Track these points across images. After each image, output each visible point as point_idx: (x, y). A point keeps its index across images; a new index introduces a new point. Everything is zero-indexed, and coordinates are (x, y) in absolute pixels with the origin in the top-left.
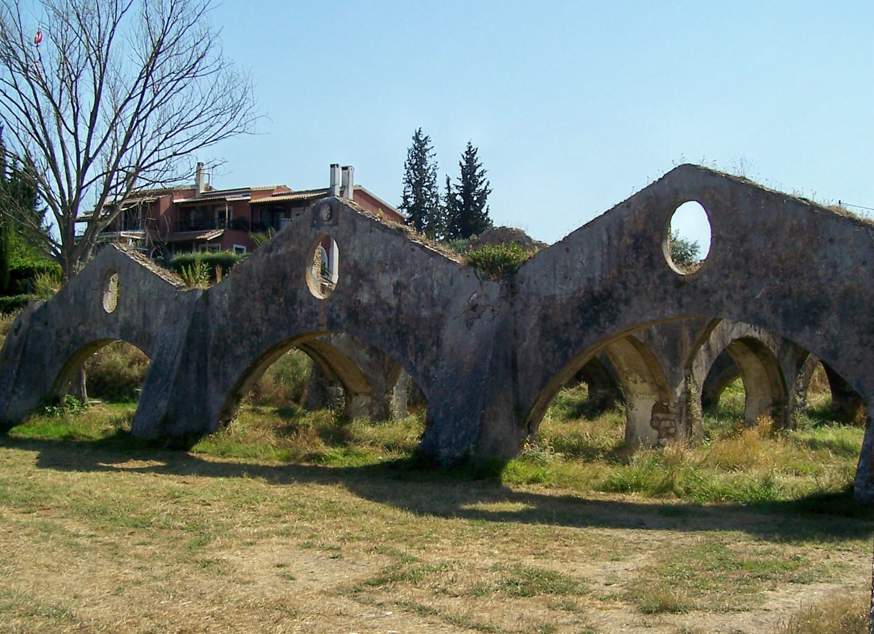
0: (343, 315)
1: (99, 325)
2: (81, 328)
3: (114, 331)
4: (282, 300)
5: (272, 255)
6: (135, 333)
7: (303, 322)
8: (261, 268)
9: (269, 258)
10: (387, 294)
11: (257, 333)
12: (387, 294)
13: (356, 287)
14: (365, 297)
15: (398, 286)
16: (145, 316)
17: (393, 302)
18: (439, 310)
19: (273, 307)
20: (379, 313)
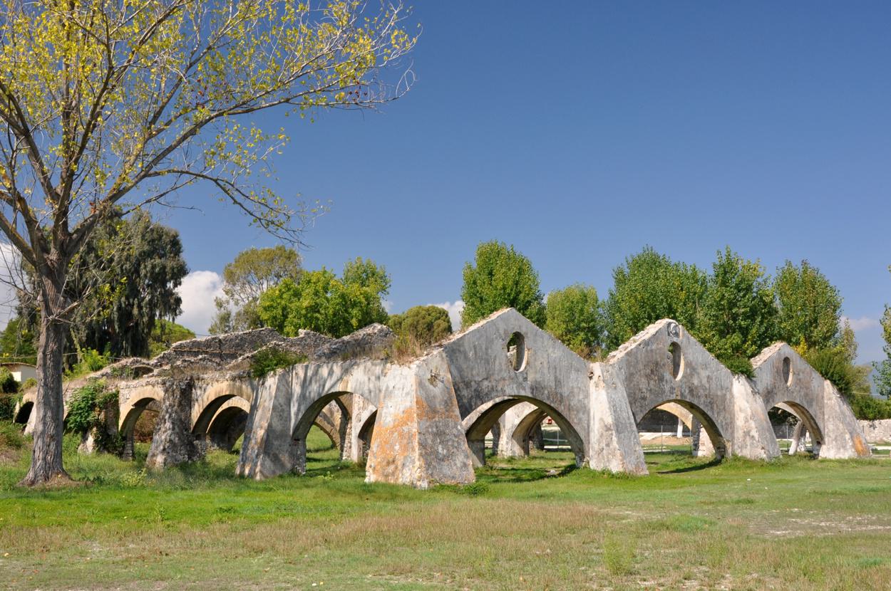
0: (687, 391)
1: (507, 382)
2: (486, 383)
3: (524, 389)
4: (656, 378)
5: (649, 348)
6: (546, 392)
7: (669, 394)
8: (643, 355)
9: (647, 351)
10: (704, 381)
11: (644, 398)
12: (704, 381)
13: (692, 375)
14: (696, 382)
15: (708, 377)
16: (556, 377)
17: (707, 386)
18: (724, 392)
19: (652, 382)
20: (702, 391)
